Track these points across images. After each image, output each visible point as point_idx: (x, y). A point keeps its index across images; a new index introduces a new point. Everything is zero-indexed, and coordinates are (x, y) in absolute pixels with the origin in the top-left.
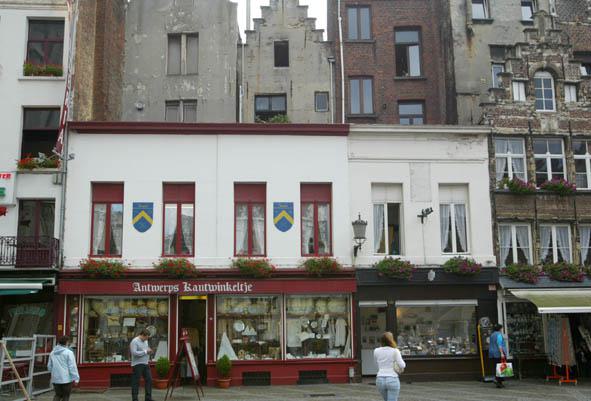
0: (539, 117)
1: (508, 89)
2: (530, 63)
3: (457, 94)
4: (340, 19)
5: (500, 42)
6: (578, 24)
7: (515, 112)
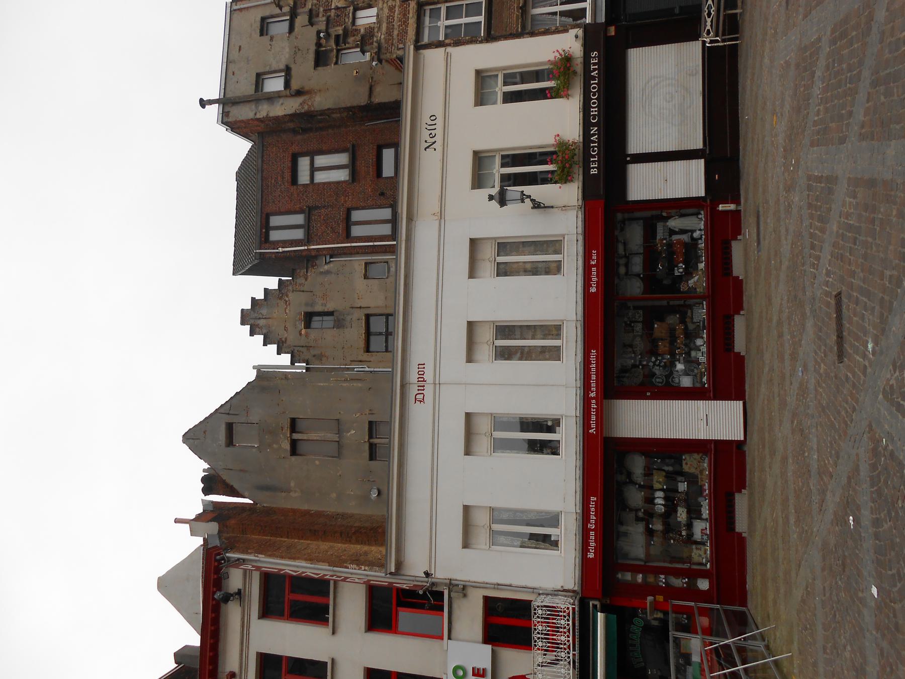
1: (362, 31)
4: (280, 250)
5: (311, 56)
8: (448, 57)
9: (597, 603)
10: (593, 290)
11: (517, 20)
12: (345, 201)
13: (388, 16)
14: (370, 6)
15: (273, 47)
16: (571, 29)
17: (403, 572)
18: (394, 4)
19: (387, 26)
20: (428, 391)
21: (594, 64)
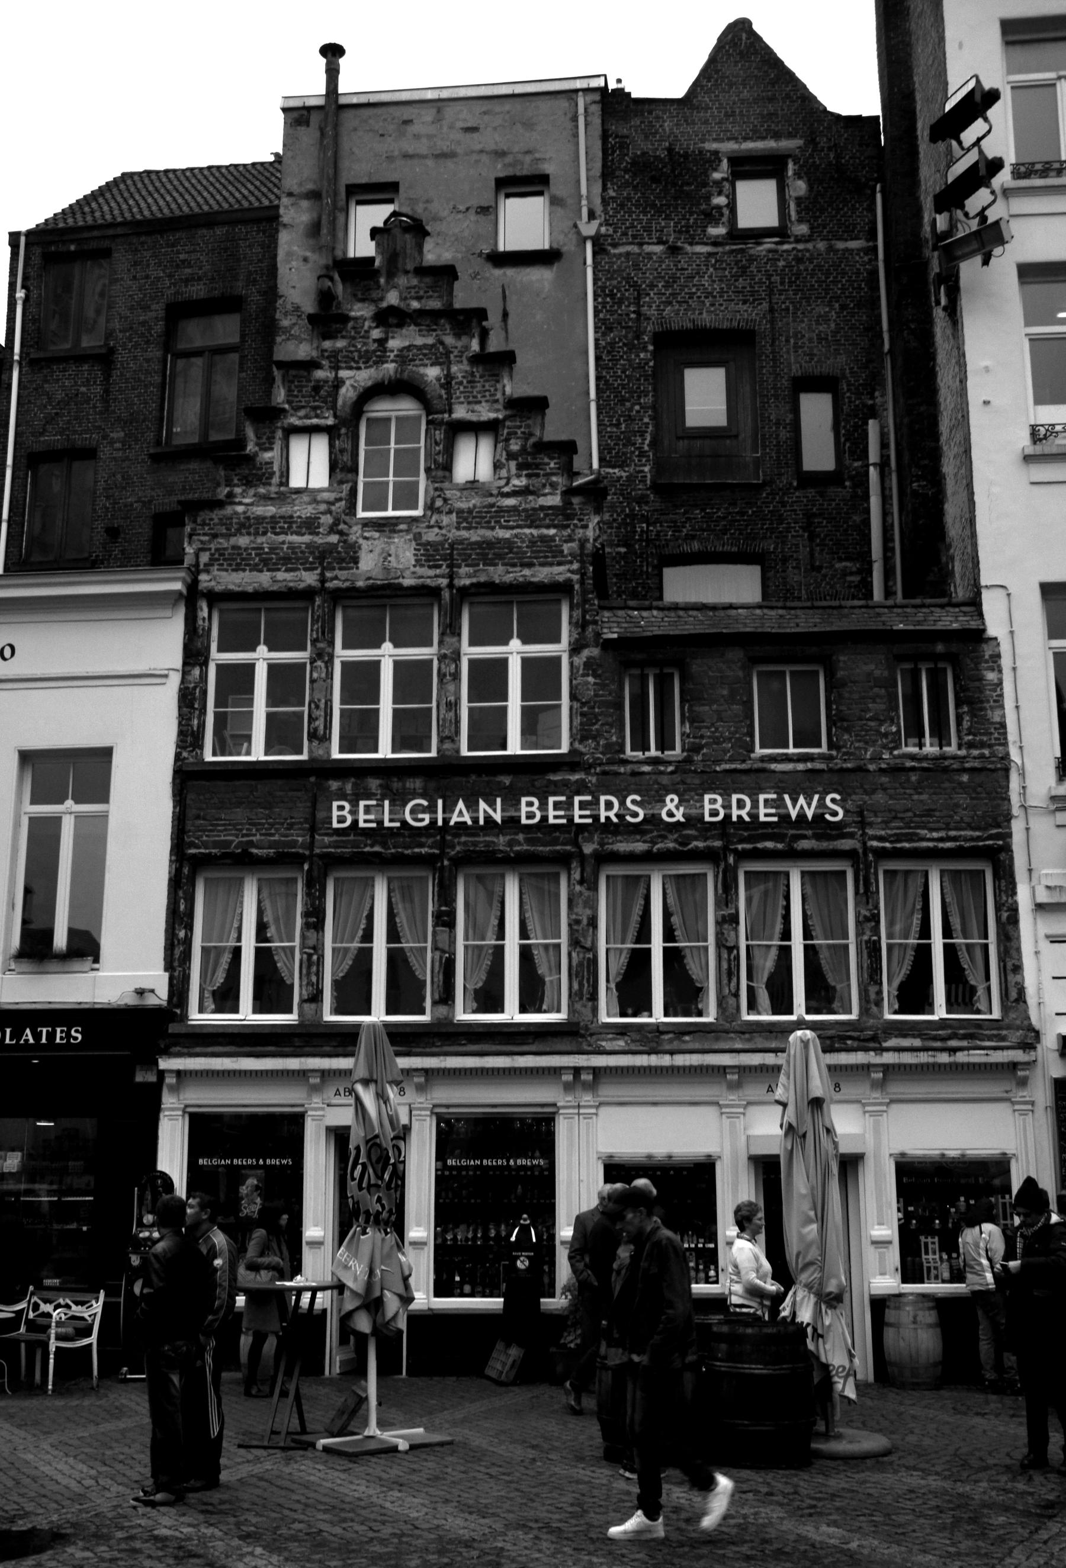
0: (355, 533)
2: (343, 374)
3: (307, 488)
6: (674, 250)
7: (289, 524)
8: (157, 677)
11: (216, 844)
12: (112, 442)
13: (291, 517)
14: (333, 466)
15: (460, 216)
16: (171, 979)
18: (321, 530)
19: (265, 518)
21: (51, 1036)
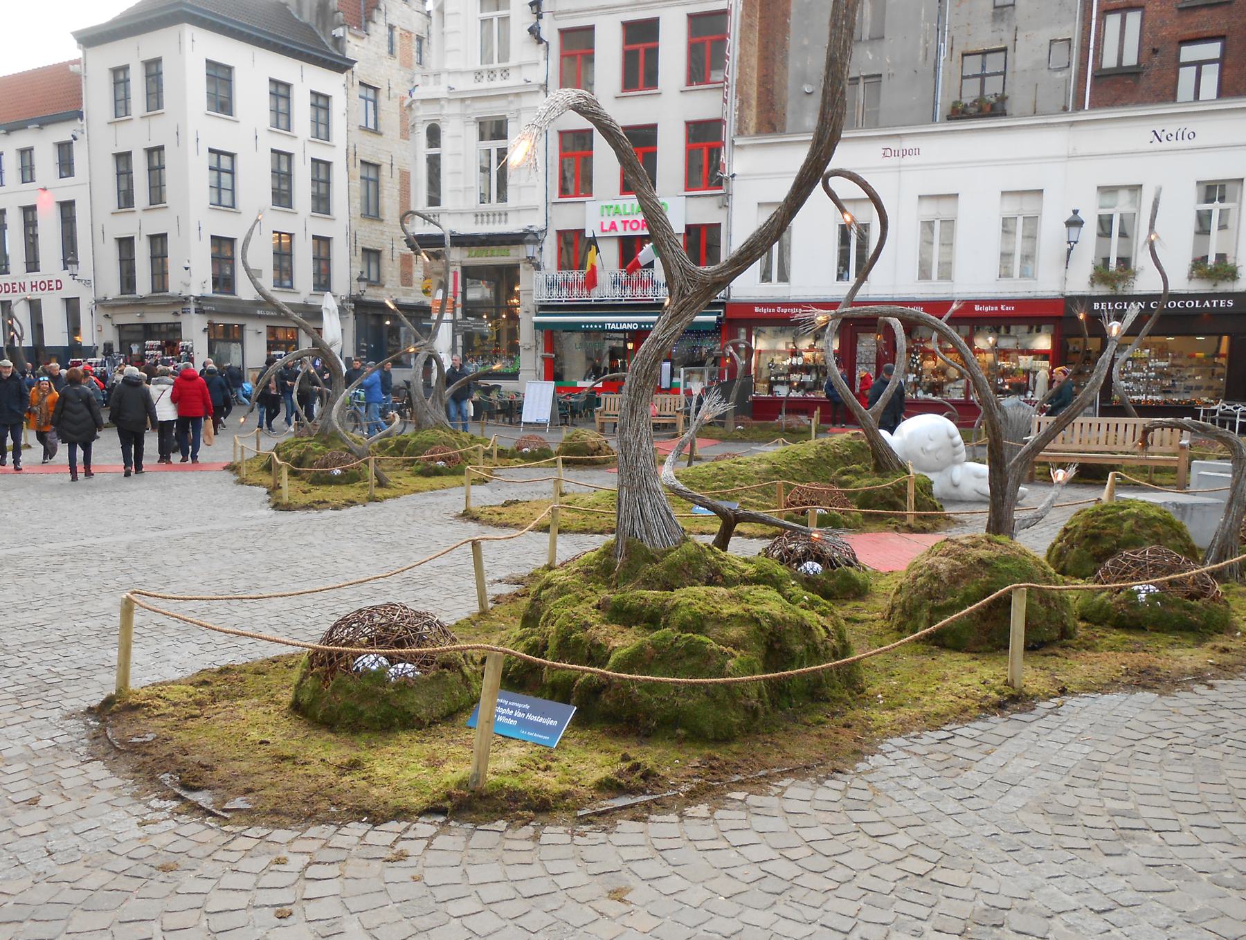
9: (722, 315)
10: (977, 308)
17: (735, 150)
20: (894, 161)
21: (1218, 304)
